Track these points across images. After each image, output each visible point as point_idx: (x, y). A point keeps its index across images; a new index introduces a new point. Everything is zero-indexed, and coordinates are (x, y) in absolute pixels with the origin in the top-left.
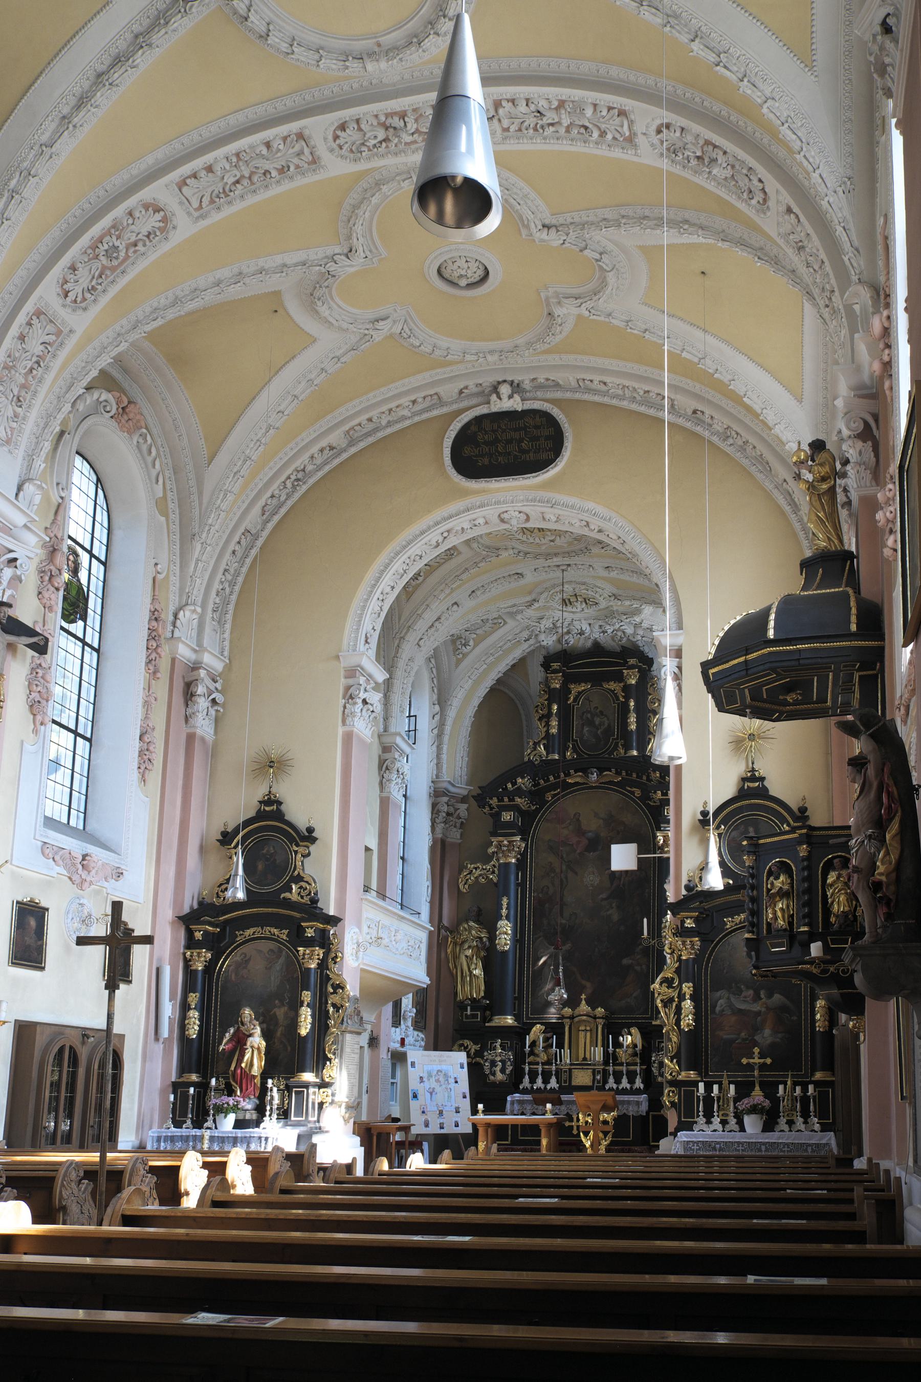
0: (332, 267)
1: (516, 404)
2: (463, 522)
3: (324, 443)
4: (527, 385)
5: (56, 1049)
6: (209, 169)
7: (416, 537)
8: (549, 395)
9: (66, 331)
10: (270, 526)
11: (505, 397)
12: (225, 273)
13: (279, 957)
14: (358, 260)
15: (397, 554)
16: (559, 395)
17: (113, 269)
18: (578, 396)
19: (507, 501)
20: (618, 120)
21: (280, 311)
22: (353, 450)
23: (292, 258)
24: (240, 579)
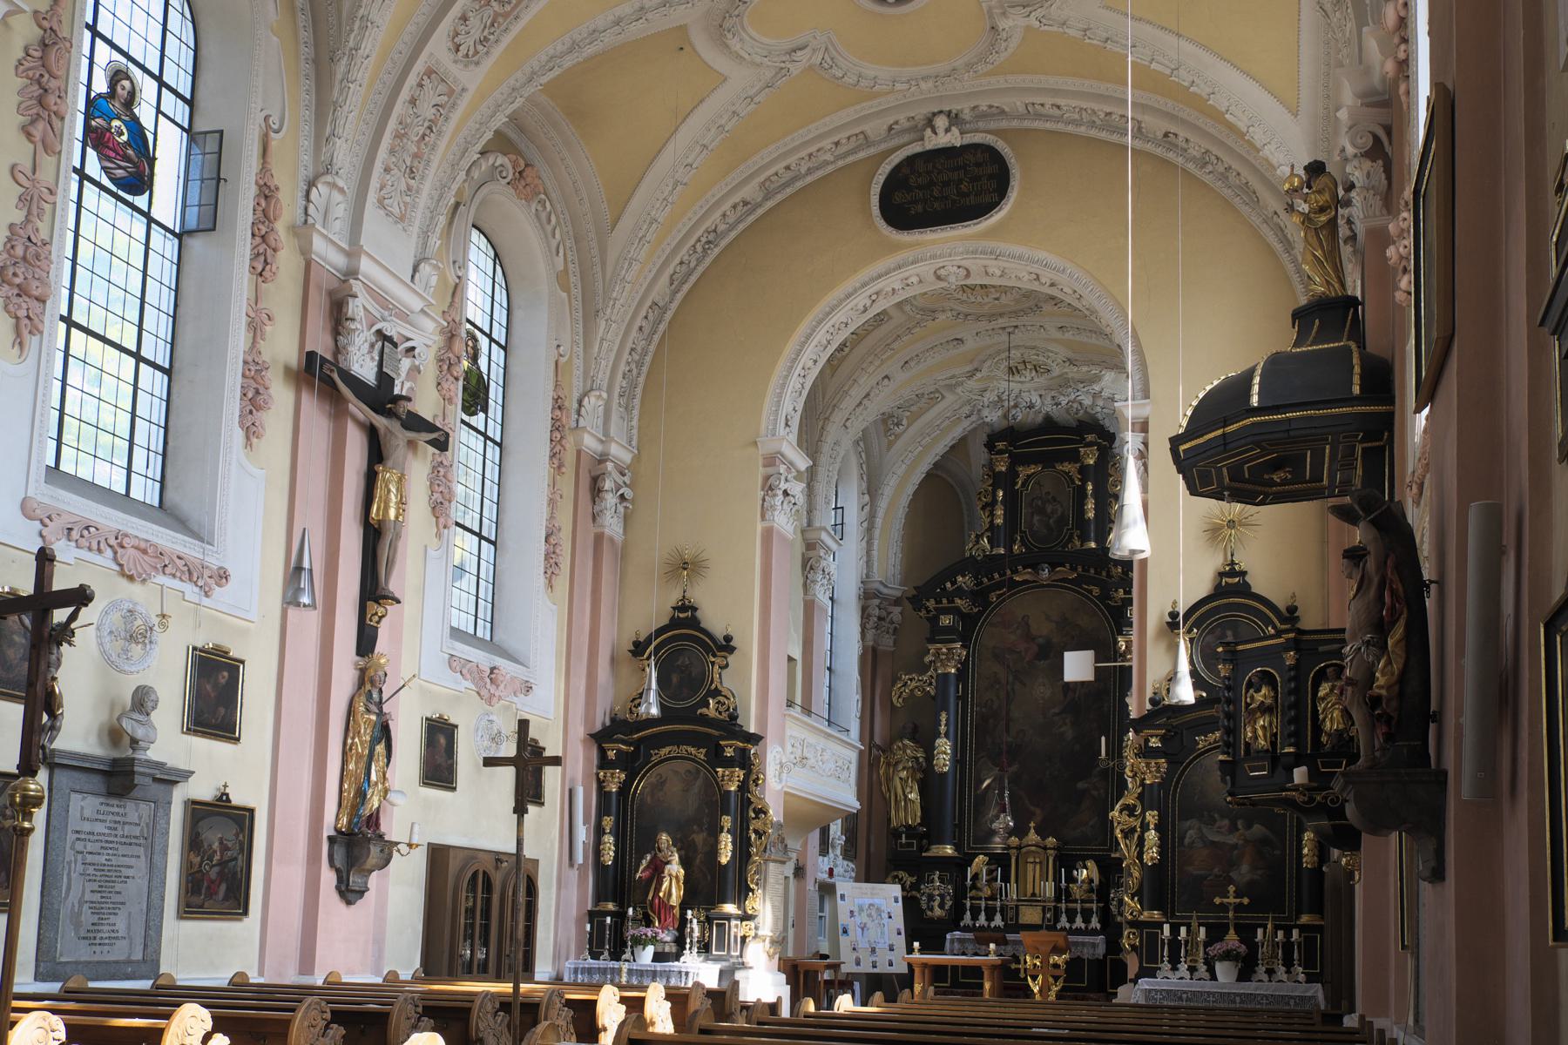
1: (954, 139)
2: (894, 282)
3: (736, 198)
5: (469, 875)
7: (841, 302)
9: (458, 89)
11: (941, 131)
12: (626, 9)
13: (696, 779)
15: (819, 322)
17: (506, 15)
19: (945, 253)
21: (687, 49)
22: (769, 204)
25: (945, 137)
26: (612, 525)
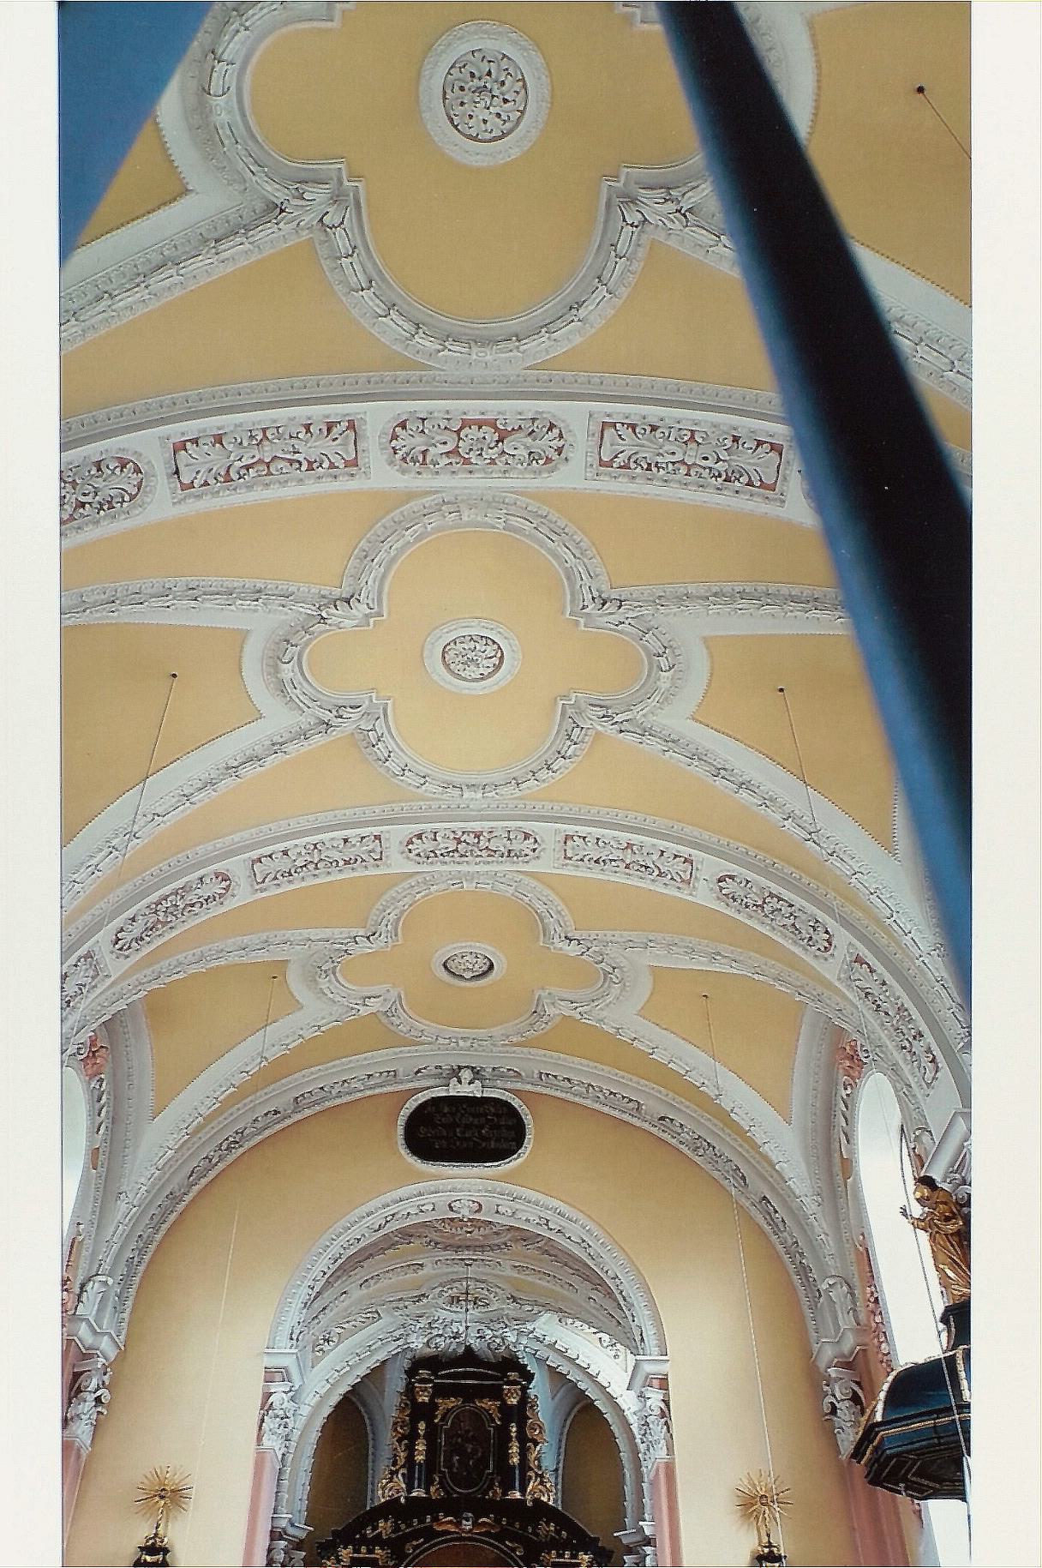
0: (351, 947)
1: (474, 1090)
4: (488, 1073)
6: (285, 853)
8: (509, 1085)
10: (196, 1188)
14: (378, 944)
16: (519, 1086)
17: (164, 924)
18: (539, 1089)
20: (682, 866)
23: (313, 933)
24: (152, 1247)
25: (466, 1088)
26: (83, 1431)
